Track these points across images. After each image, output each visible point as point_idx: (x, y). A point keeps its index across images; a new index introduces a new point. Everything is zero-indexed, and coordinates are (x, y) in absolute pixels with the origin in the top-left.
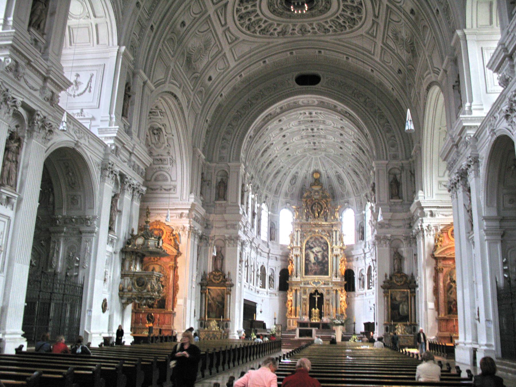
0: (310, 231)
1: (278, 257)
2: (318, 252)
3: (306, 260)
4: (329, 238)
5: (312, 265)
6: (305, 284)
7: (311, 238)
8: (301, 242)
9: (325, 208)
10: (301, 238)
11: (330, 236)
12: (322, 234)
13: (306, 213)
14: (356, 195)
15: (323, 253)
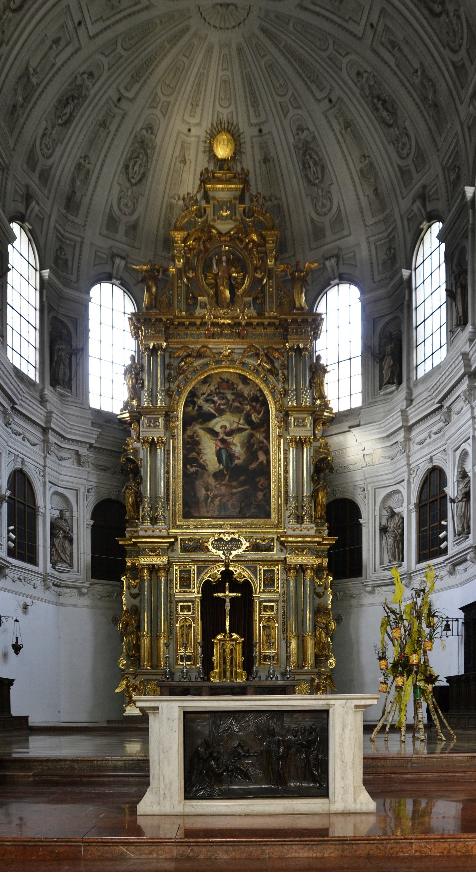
0: (200, 355)
1: (83, 451)
2: (231, 433)
3: (187, 461)
4: (271, 376)
5: (212, 481)
6: (185, 549)
7: (205, 381)
8: (168, 393)
9: (256, 269)
10: (168, 379)
11: (273, 372)
12: (243, 364)
13: (187, 286)
14: (370, 221)
15: (251, 436)
